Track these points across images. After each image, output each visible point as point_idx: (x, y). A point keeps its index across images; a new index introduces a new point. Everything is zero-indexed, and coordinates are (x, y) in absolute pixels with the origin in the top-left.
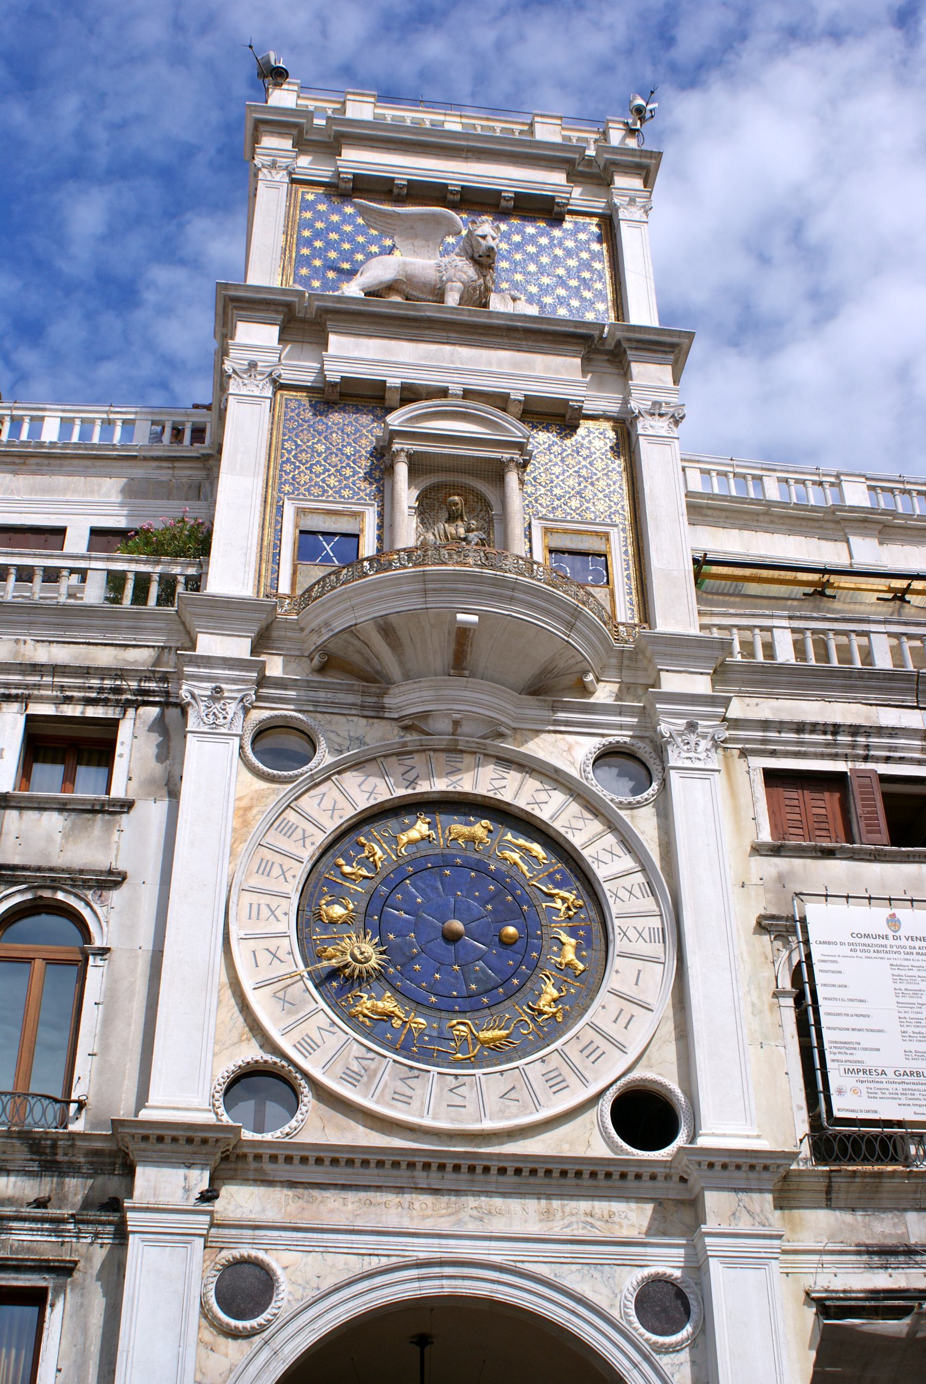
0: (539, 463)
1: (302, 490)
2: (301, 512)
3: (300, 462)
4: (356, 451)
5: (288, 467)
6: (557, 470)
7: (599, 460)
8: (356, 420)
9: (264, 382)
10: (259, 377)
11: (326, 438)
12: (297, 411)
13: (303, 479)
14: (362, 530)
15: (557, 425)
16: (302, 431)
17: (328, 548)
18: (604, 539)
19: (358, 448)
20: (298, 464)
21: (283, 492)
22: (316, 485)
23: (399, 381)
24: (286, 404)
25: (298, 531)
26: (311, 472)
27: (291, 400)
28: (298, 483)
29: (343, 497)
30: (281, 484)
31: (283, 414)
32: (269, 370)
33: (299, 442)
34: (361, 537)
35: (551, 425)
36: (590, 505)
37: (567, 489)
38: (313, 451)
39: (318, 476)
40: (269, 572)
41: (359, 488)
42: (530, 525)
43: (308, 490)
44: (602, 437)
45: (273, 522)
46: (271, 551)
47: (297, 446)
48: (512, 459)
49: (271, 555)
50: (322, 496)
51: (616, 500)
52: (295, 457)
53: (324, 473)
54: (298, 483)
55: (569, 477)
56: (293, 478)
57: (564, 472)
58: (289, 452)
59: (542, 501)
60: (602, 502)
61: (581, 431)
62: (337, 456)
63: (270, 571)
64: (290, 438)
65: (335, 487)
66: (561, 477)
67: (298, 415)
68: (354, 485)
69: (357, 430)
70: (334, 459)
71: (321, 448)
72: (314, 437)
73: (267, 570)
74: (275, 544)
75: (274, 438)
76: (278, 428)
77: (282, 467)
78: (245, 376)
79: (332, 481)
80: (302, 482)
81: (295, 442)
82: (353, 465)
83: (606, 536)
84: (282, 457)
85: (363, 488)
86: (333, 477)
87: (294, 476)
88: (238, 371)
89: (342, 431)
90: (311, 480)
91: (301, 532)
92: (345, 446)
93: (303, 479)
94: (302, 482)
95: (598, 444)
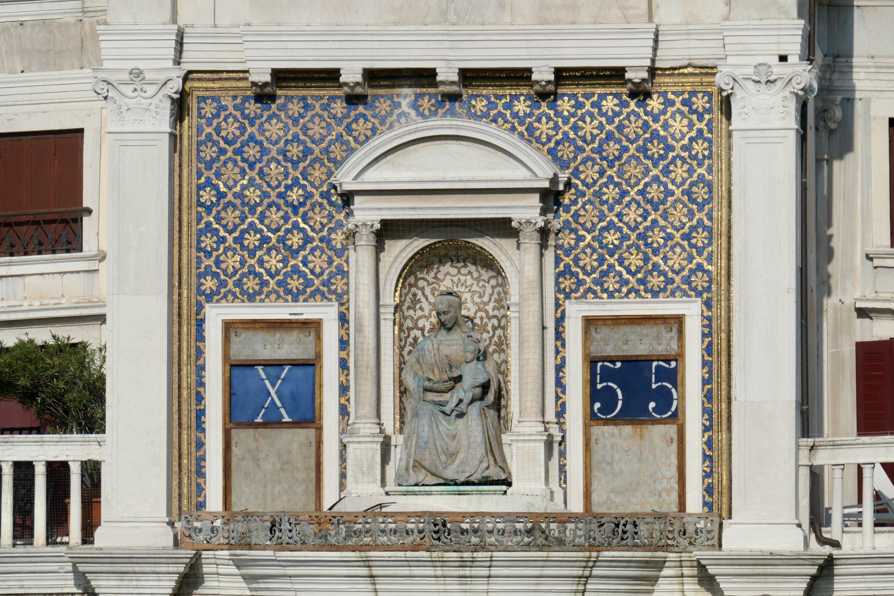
0: (583, 182)
1: (230, 282)
2: (229, 327)
3: (225, 227)
4: (308, 196)
5: (208, 242)
6: (611, 193)
7: (679, 163)
8: (305, 129)
9: (156, 101)
10: (151, 90)
11: (261, 174)
12: (215, 122)
13: (232, 261)
14: (319, 356)
15: (615, 95)
16: (225, 163)
17: (273, 392)
18: (675, 330)
19: (309, 189)
20: (222, 233)
21: (203, 293)
22: (250, 272)
23: (359, 67)
24: (199, 109)
25: (228, 368)
26: (243, 247)
27: (204, 99)
28: (225, 272)
29: (289, 292)
30: (199, 276)
31: (195, 130)
32: (163, 77)
33: (223, 189)
34: (318, 370)
35: (603, 97)
36: (658, 259)
37: (625, 230)
38: (243, 204)
39: (252, 254)
40: (193, 449)
41: (312, 272)
42: (563, 312)
43: (239, 284)
44: (685, 109)
45: (193, 351)
46: (194, 407)
47: (221, 195)
48: (528, 222)
49: (194, 415)
50: (260, 293)
51: (700, 244)
52: (218, 219)
53: (260, 247)
54: (225, 272)
55: (628, 205)
56: (218, 263)
57: (624, 193)
58: (209, 210)
59: (586, 260)
60: (678, 250)
61: (655, 104)
62: (278, 210)
63: (194, 444)
64: (209, 182)
65: (278, 272)
66: (618, 208)
67: (218, 130)
68: (305, 265)
69: (307, 152)
70: (275, 216)
71: (253, 195)
72: (243, 172)
73: (189, 444)
74: (198, 394)
75: (185, 185)
76: (190, 160)
77: (199, 242)
78: (128, 90)
79: (273, 262)
80: (230, 270)
81: (216, 187)
82: (302, 225)
83: (679, 320)
84: (199, 221)
85: (318, 270)
86: (274, 253)
87: (218, 257)
88: (115, 84)
89: (285, 156)
90: (243, 263)
91: (231, 365)
92: (289, 188)
93: (232, 261)
94: (230, 270)
95: (678, 125)
